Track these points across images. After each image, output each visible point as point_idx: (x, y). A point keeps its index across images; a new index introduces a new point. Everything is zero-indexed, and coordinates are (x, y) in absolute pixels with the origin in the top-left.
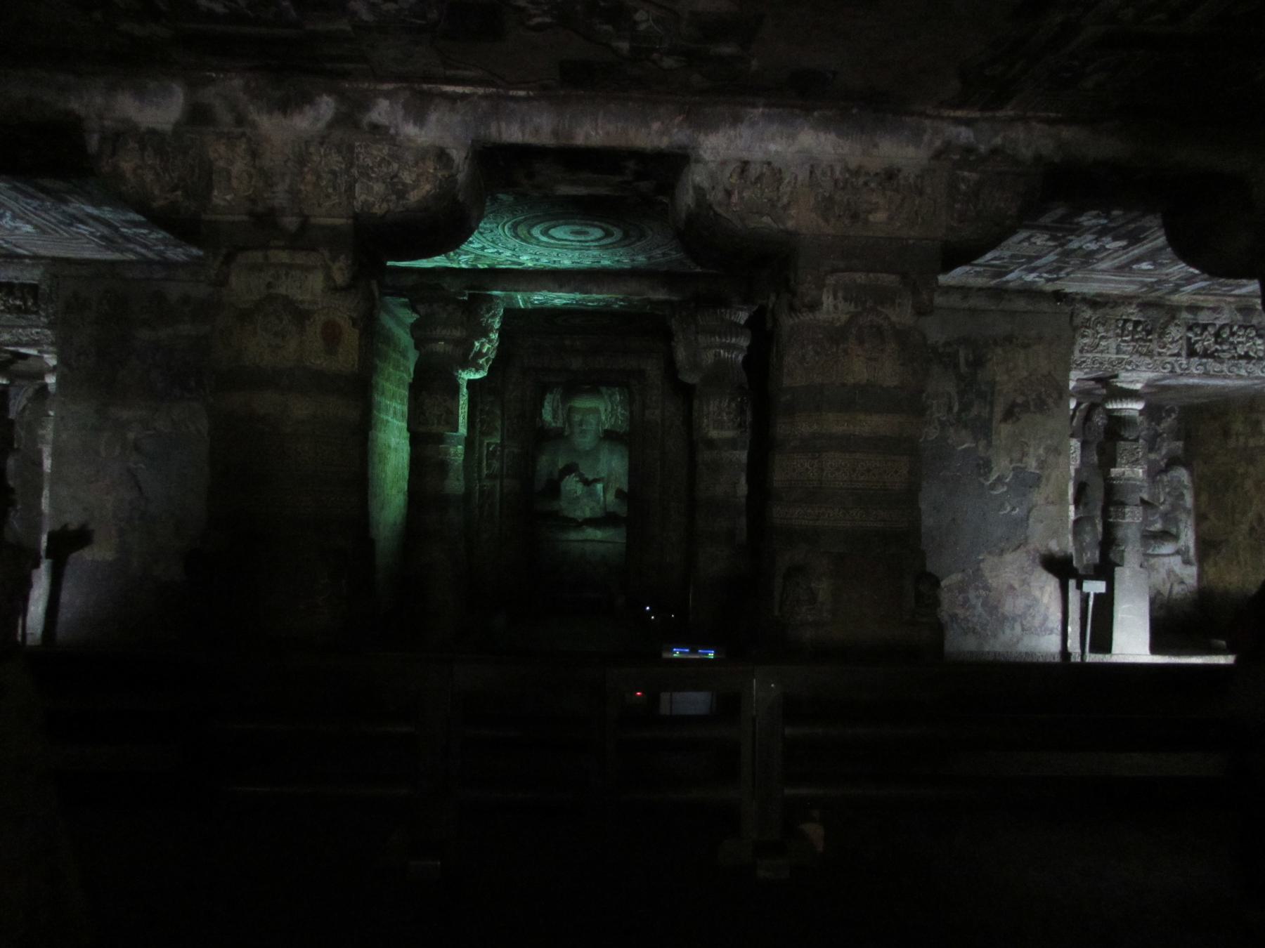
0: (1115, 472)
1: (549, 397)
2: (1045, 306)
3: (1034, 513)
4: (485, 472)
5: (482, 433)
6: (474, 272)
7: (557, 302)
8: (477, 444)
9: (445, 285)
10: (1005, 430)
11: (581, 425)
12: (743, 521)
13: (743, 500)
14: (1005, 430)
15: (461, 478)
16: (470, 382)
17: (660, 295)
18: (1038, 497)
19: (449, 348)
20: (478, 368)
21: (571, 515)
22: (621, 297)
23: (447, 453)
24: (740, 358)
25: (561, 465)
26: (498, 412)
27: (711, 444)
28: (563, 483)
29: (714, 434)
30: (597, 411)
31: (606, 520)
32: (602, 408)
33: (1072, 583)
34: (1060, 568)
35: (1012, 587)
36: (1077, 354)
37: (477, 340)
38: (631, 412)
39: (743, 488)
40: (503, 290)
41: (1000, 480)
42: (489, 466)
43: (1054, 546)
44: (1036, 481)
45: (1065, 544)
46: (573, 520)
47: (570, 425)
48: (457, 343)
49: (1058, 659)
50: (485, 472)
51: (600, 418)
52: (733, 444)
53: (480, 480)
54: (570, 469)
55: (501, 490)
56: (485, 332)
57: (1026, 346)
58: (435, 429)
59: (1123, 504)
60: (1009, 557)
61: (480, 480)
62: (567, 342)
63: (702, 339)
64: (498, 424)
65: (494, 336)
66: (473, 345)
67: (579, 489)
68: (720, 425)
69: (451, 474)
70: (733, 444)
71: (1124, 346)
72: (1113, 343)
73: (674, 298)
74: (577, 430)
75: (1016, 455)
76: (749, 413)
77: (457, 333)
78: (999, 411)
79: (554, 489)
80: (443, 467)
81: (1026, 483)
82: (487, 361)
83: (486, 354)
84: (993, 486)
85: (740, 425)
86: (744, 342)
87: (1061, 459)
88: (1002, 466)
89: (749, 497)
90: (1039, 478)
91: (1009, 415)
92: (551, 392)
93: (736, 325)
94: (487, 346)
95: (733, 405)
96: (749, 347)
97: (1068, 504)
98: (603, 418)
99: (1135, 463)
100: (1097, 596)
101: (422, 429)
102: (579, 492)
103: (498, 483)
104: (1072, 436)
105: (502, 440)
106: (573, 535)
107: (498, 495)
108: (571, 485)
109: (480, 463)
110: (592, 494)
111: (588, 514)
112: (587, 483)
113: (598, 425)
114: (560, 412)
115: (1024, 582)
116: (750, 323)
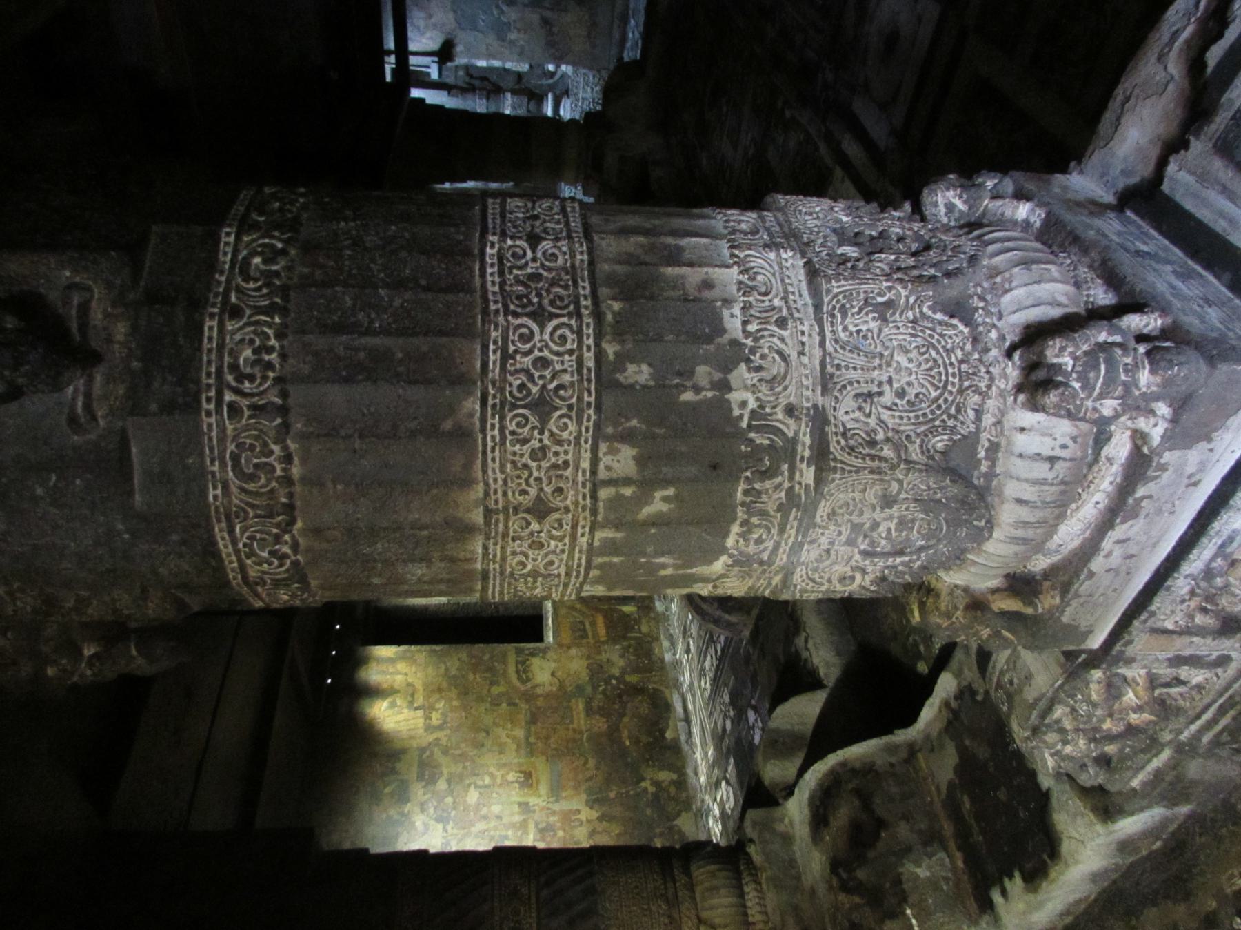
0: (509, 95)
2: (614, 51)
3: (480, 36)
10: (534, 17)
14: (534, 17)
18: (491, 39)
33: (436, 59)
34: (445, 53)
35: (430, 16)
36: (583, 71)
41: (502, 12)
43: (459, 48)
44: (501, 38)
45: (460, 60)
49: (386, 47)
57: (589, 36)
59: (488, 99)
60: (451, 16)
71: (586, 103)
72: (588, 95)
75: (518, 25)
78: (548, 14)
81: (501, 31)
84: (498, 6)
87: (516, 57)
88: (512, 14)
90: (503, 40)
91: (545, 22)
97: (488, 60)
99: (514, 108)
100: (428, 74)
104: (531, 67)
115: (435, 26)
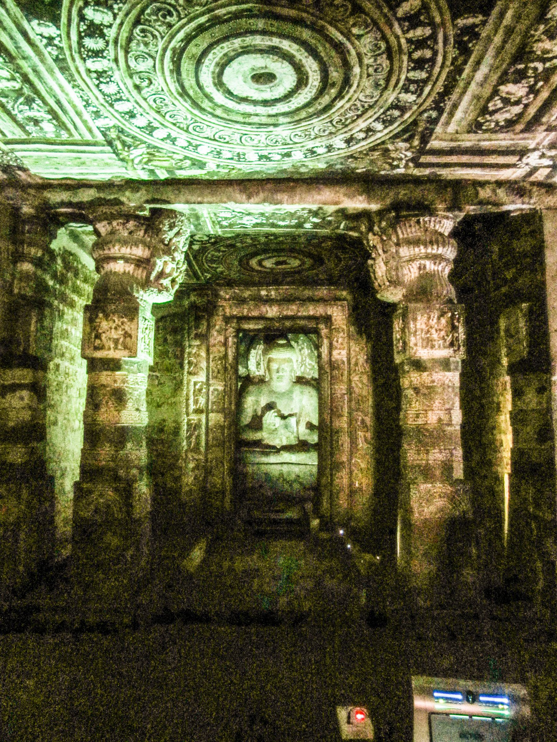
1: (253, 352)
4: (192, 407)
5: (190, 373)
6: (155, 183)
7: (249, 222)
8: (185, 382)
9: (123, 199)
11: (278, 372)
12: (459, 453)
13: (458, 428)
15: (144, 407)
16: (156, 307)
17: (357, 203)
19: (130, 268)
20: (161, 289)
21: (271, 443)
22: (314, 207)
23: (124, 382)
24: (447, 271)
25: (263, 402)
26: (203, 354)
27: (418, 365)
28: (264, 419)
29: (423, 354)
30: (290, 360)
31: (302, 446)
32: (294, 360)
37: (160, 257)
38: (319, 356)
39: (457, 416)
40: (187, 202)
42: (196, 402)
46: (274, 447)
47: (270, 374)
48: (140, 263)
50: (192, 407)
51: (292, 366)
52: (445, 364)
53: (188, 414)
54: (270, 407)
55: (207, 423)
56: (168, 250)
58: (111, 354)
61: (188, 414)
62: (263, 293)
63: (405, 252)
64: (204, 364)
65: (180, 257)
66: (155, 264)
67: (278, 422)
68: (429, 343)
69: (130, 404)
70: (445, 364)
73: (374, 207)
74: (275, 376)
76: (461, 330)
77: (140, 252)
79: (257, 423)
80: (119, 397)
82: (173, 281)
83: (170, 275)
85: (452, 344)
86: (450, 252)
89: (463, 426)
92: (255, 349)
93: (441, 234)
94: (173, 267)
95: (443, 321)
96: (456, 261)
98: (295, 366)
101: (99, 354)
102: (277, 426)
103: (203, 417)
105: (208, 376)
106: (272, 459)
107: (203, 427)
108: (270, 419)
109: (187, 400)
110: (286, 427)
111: (285, 443)
112: (283, 417)
113: (291, 371)
114: (262, 363)
116: (455, 234)
